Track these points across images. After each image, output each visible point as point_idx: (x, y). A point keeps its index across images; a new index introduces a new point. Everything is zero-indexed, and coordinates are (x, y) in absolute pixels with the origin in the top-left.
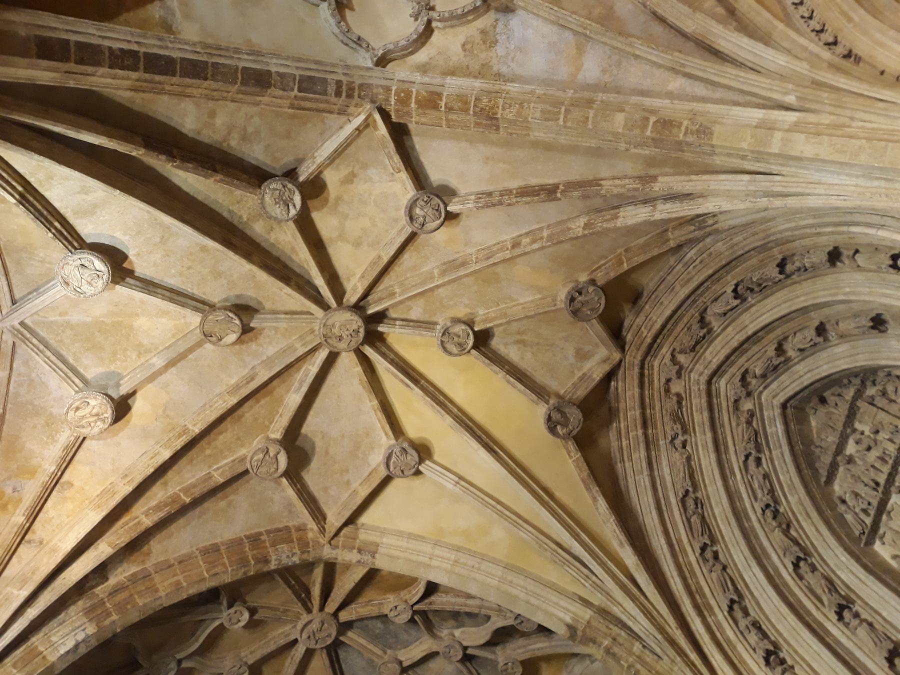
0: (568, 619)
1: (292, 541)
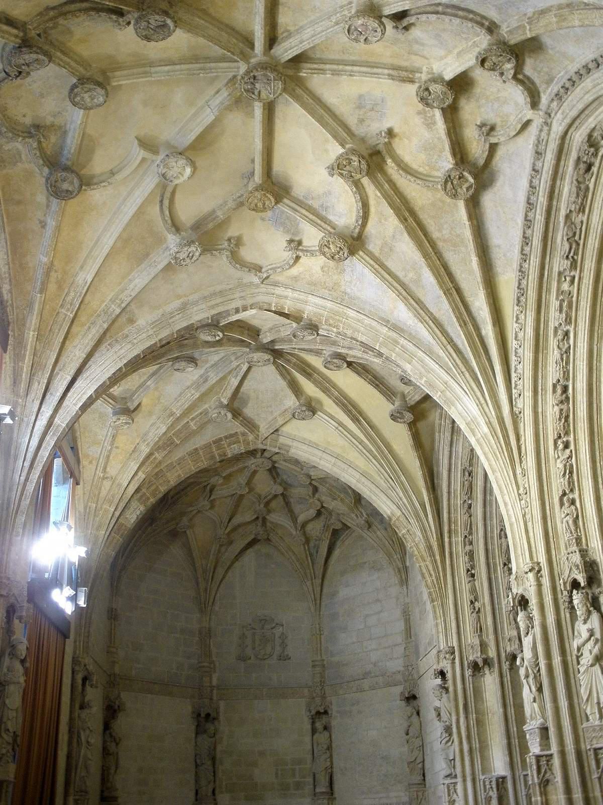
0: (389, 512)
1: (240, 442)
